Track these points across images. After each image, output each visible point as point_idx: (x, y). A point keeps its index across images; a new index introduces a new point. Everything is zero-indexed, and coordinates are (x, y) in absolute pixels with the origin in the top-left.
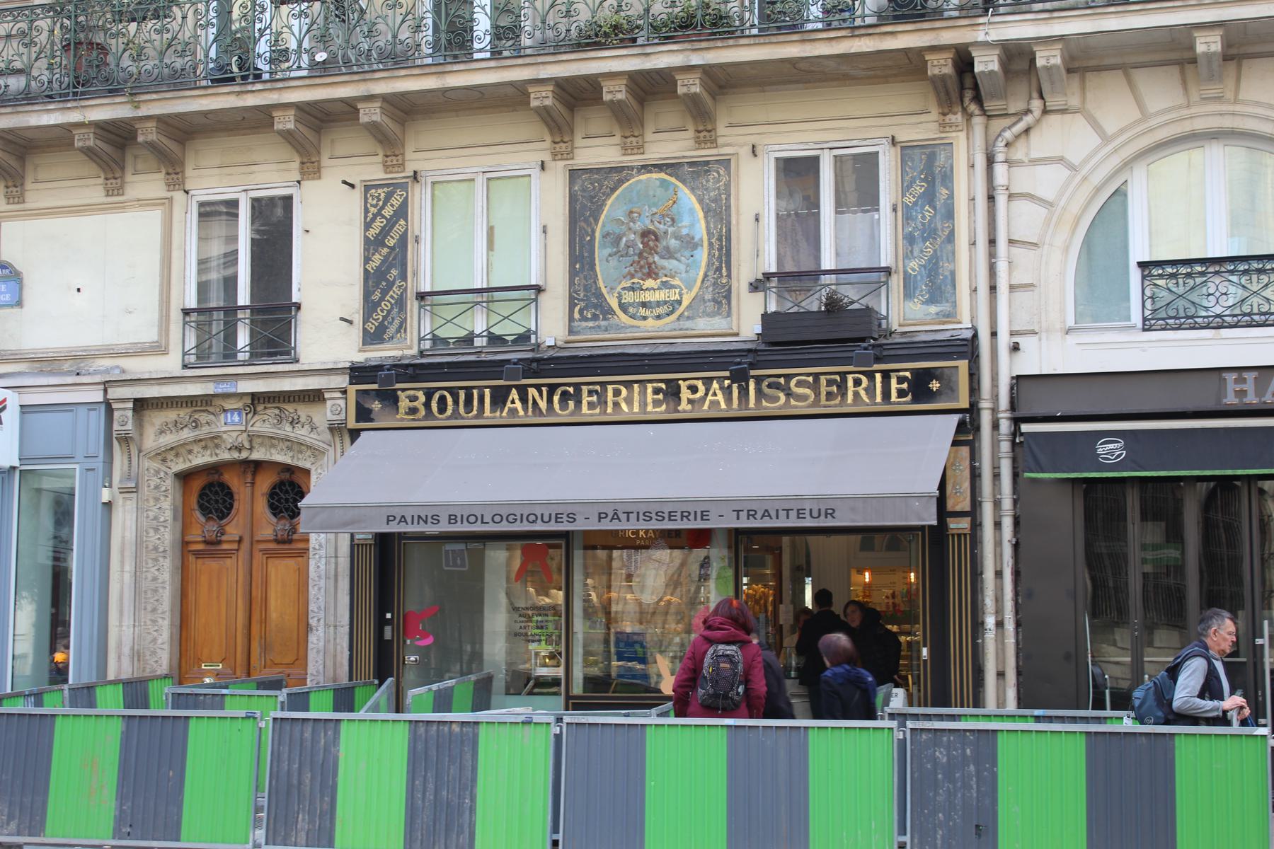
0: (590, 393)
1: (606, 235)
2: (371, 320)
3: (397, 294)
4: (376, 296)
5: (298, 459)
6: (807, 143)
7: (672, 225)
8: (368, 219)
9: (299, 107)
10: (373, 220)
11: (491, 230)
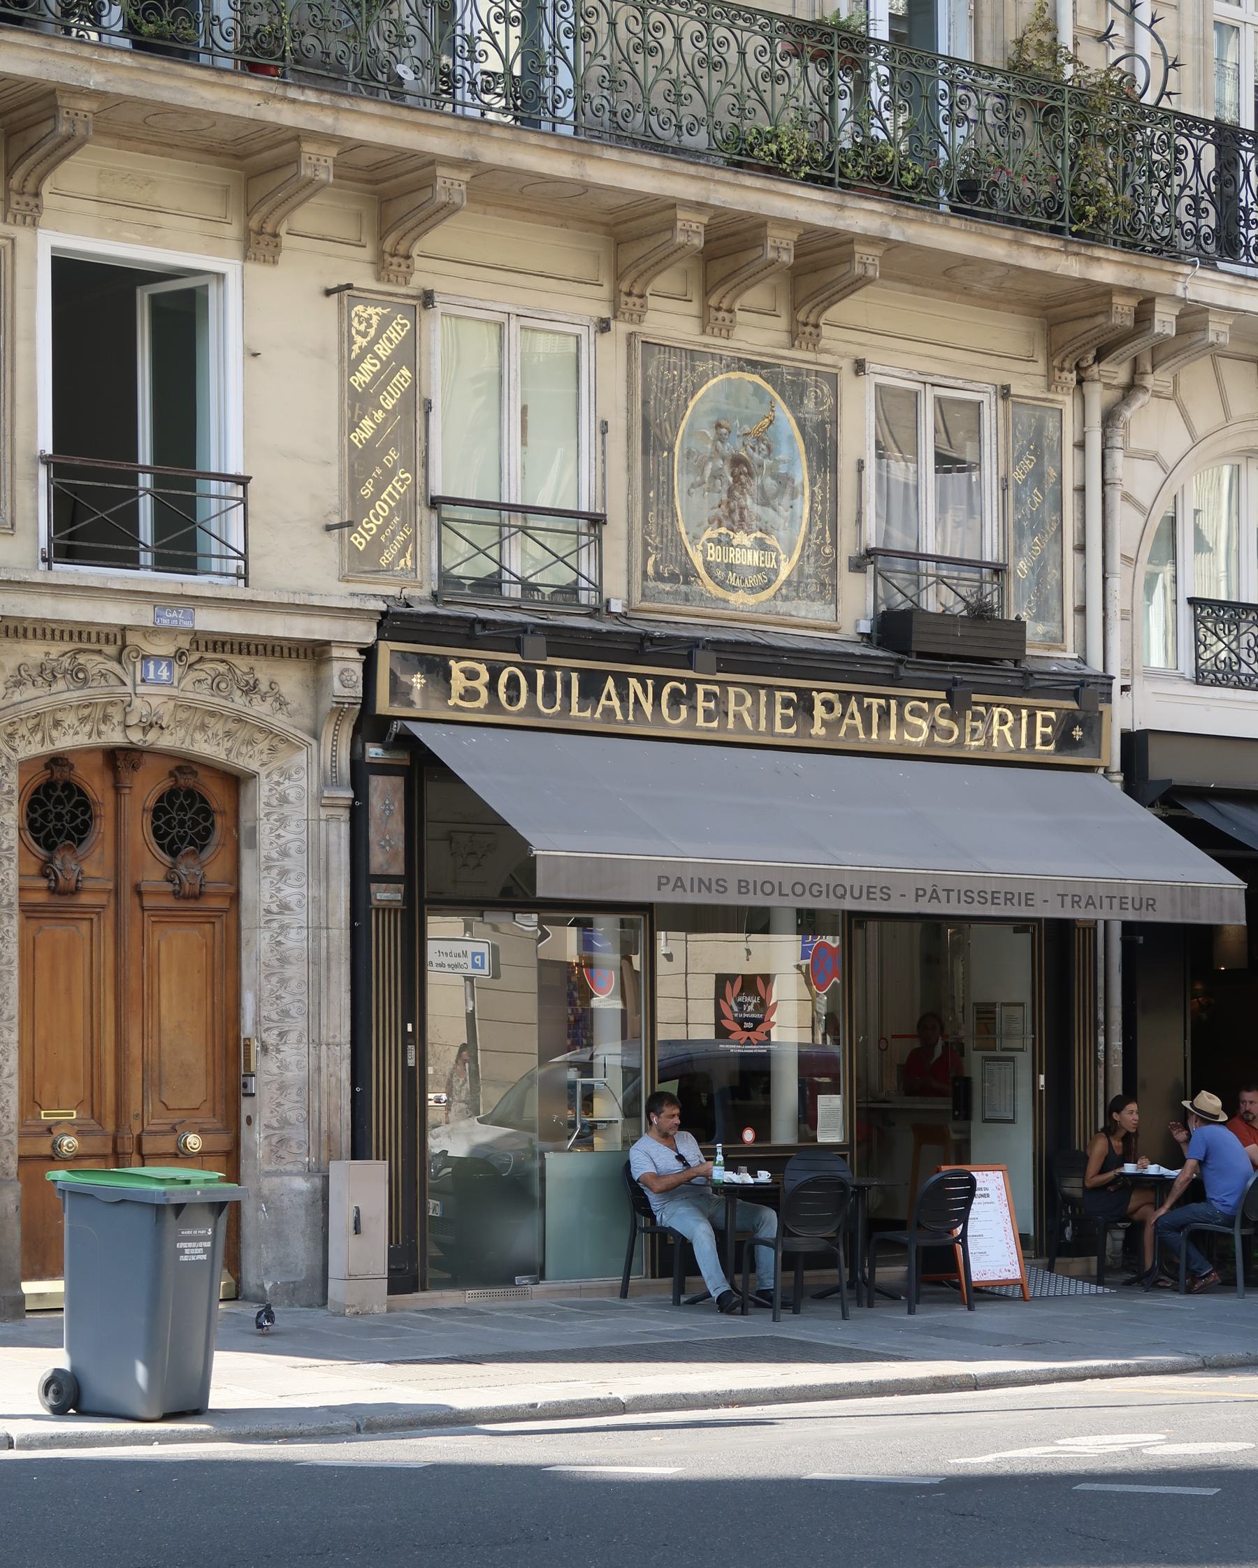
0: (708, 696)
1: (689, 454)
2: (359, 529)
3: (399, 493)
4: (367, 491)
5: (239, 754)
6: (911, 371)
7: (768, 456)
8: (353, 356)
9: (349, 146)
10: (361, 358)
11: (524, 410)
